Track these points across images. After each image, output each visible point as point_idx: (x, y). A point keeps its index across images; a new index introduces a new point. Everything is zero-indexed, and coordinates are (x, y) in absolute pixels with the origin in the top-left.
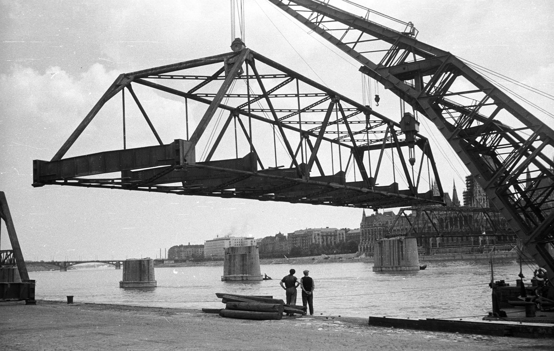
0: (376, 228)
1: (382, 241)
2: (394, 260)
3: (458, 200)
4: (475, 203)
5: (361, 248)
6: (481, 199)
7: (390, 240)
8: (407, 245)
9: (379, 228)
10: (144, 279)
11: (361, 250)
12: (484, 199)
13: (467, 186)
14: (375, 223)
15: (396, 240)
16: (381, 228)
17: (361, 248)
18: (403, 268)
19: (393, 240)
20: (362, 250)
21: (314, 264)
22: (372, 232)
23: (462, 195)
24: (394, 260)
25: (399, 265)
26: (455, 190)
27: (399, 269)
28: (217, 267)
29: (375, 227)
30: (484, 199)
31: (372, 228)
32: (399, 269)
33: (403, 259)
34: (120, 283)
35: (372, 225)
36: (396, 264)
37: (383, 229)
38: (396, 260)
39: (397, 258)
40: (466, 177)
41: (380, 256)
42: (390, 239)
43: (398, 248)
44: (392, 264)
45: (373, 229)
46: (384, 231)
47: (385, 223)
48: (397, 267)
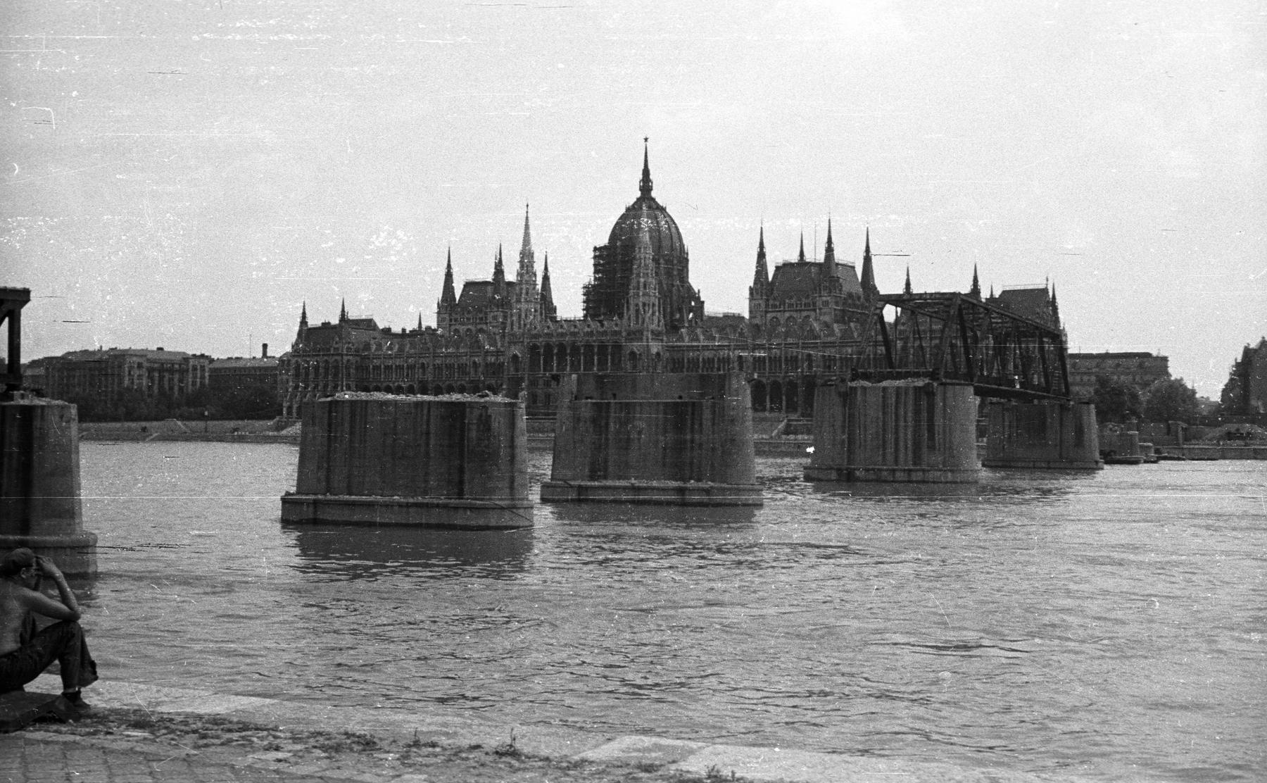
0: (339, 358)
1: (854, 389)
2: (897, 450)
3: (552, 304)
4: (630, 312)
5: (290, 408)
6: (649, 305)
7: (885, 389)
8: (951, 402)
9: (345, 358)
10: (492, 491)
11: (289, 412)
12: (654, 305)
13: (596, 272)
14: (337, 346)
15: (907, 389)
16: (351, 358)
17: (290, 408)
18: (932, 475)
19: (898, 388)
20: (295, 415)
21: (153, 440)
22: (327, 369)
23: (581, 291)
24: (897, 450)
25: (915, 464)
26: (867, 260)
27: (917, 476)
28: (119, 442)
29: (338, 355)
30: (654, 305)
31: (326, 358)
32: (914, 477)
33: (932, 448)
34: (284, 501)
35: (329, 350)
36: (906, 461)
37: (357, 362)
38: (906, 448)
39: (910, 443)
40: (595, 249)
41: (843, 432)
42: (885, 384)
43: (917, 412)
44: (890, 458)
45: (332, 360)
46: (357, 369)
47: (361, 347)
48: (910, 471)
